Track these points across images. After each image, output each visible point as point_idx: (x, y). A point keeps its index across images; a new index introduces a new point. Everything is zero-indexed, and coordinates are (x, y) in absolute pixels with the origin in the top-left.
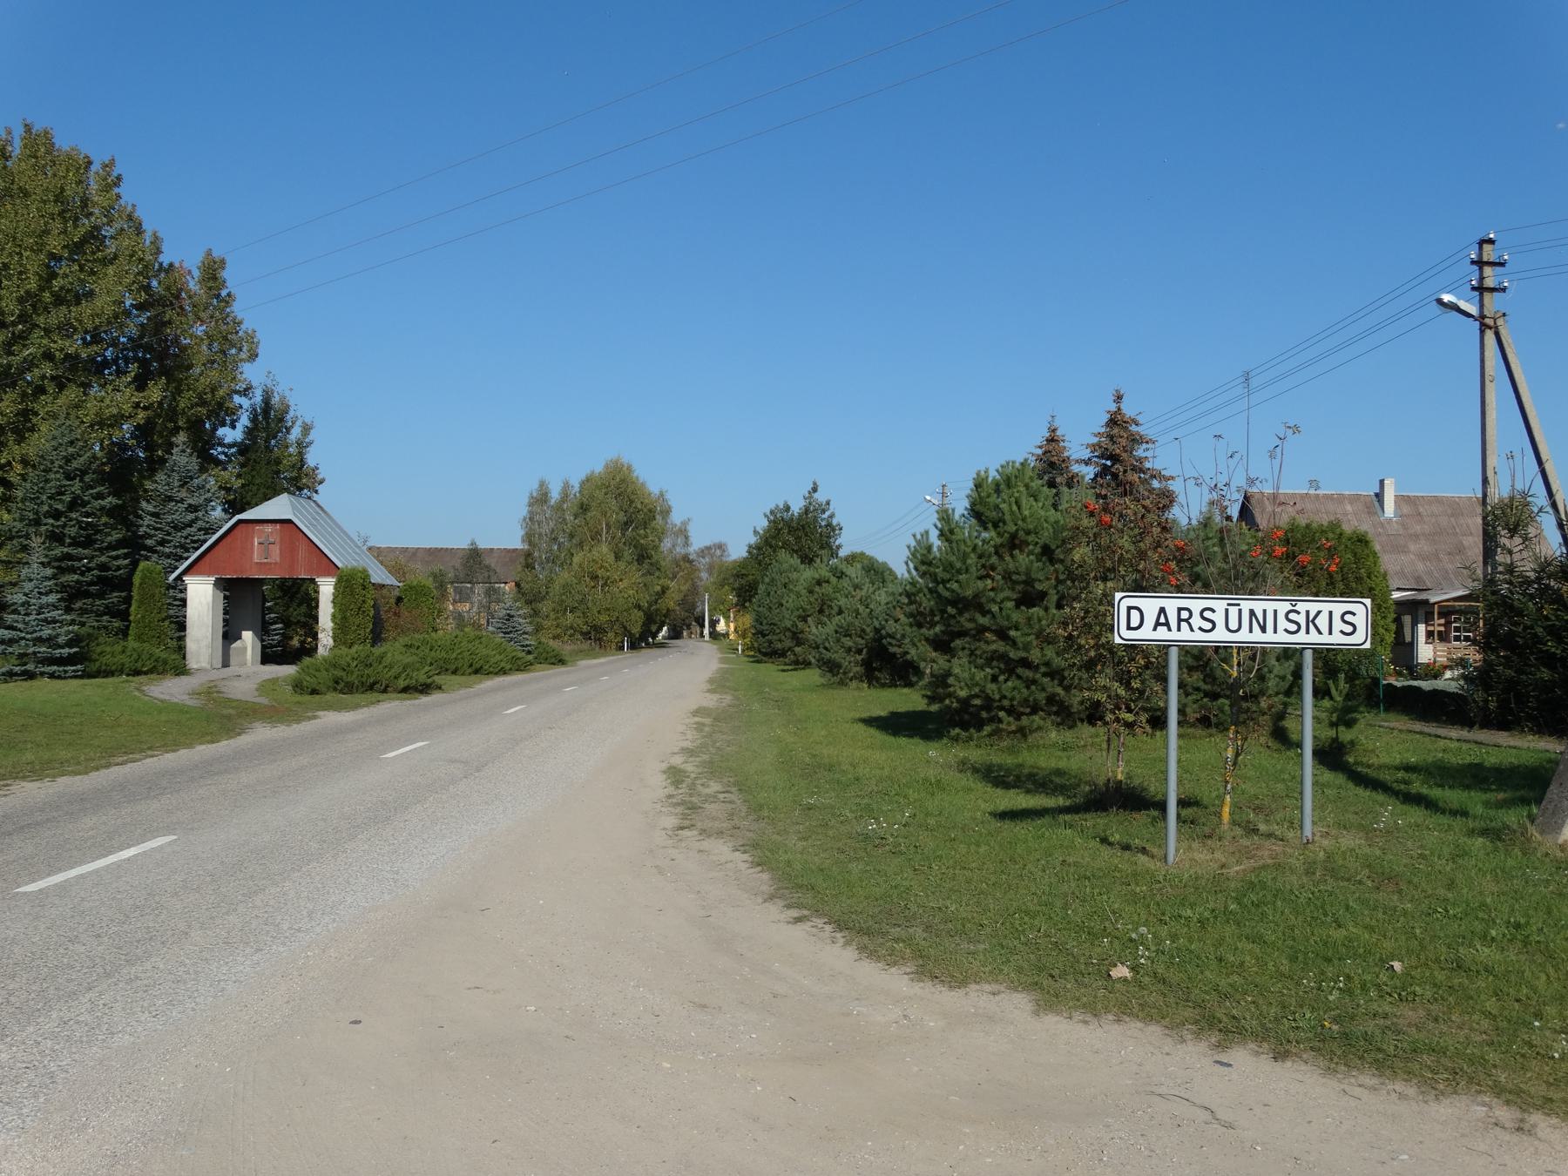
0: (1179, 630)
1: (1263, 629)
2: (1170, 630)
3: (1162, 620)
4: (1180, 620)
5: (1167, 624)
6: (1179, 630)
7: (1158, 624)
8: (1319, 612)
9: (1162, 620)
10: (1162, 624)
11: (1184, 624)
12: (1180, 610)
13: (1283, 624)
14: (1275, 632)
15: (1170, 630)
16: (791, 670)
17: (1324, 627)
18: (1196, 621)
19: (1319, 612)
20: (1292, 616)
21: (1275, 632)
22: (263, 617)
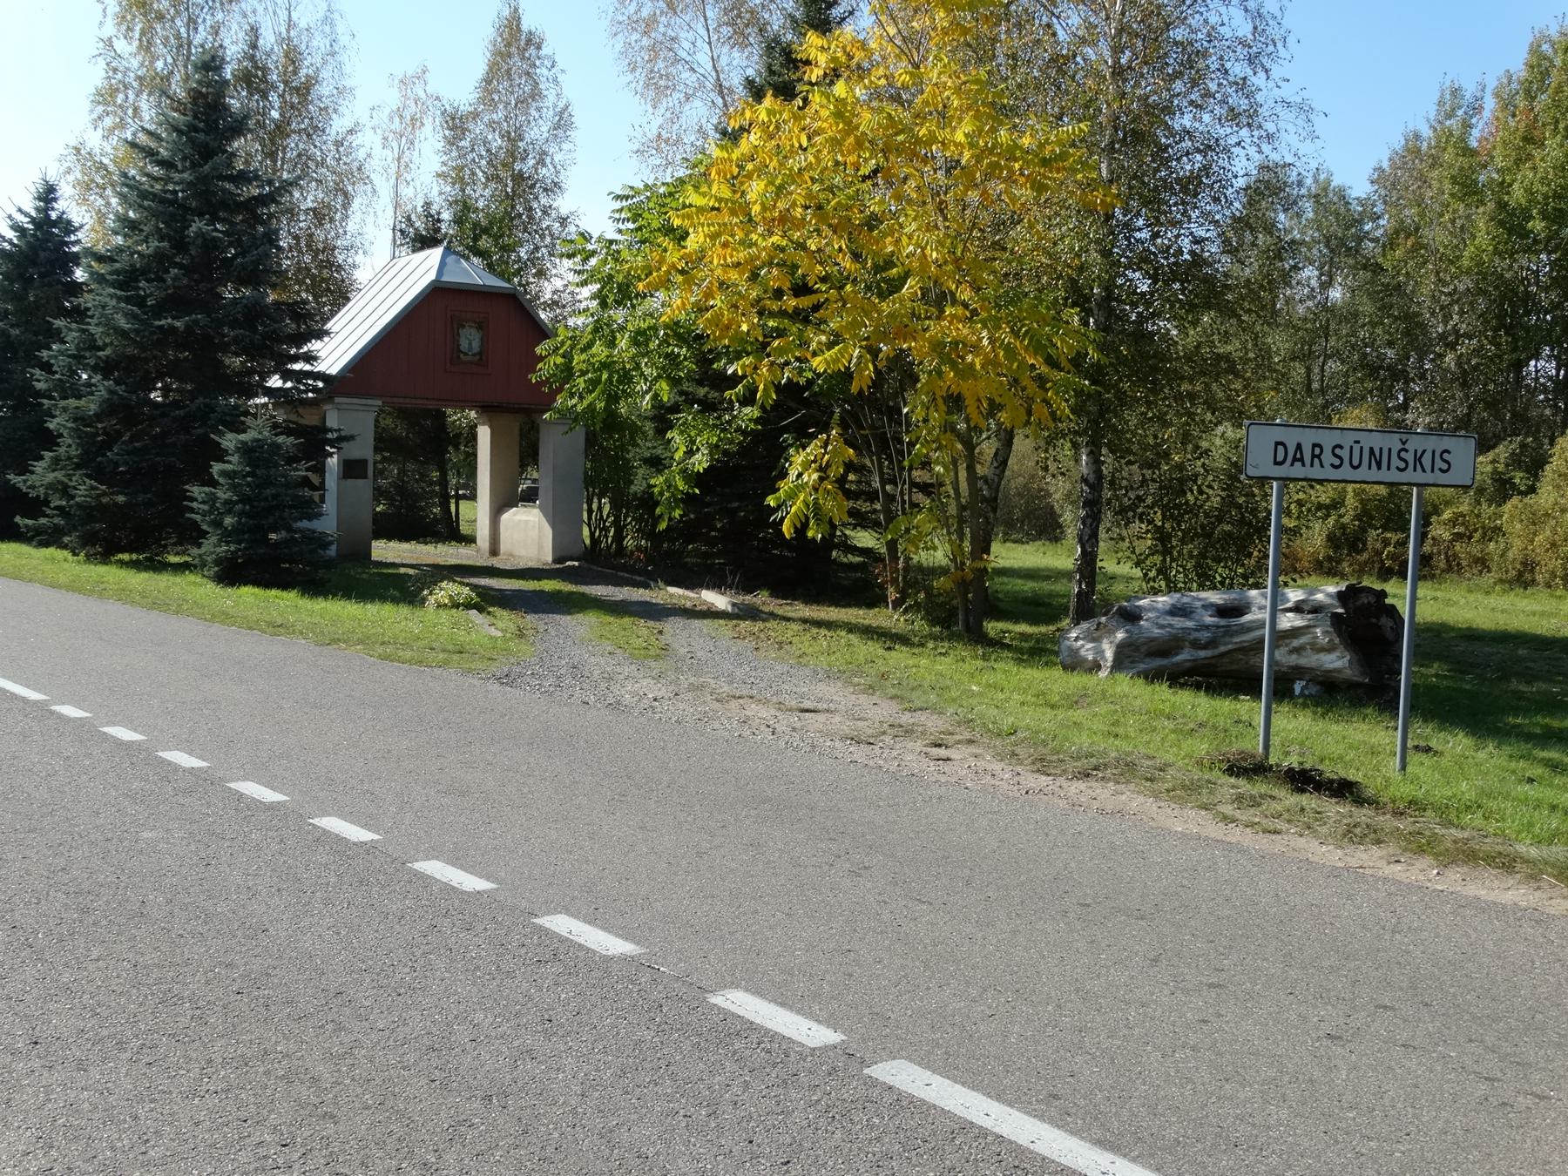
0: (1312, 465)
1: (1379, 467)
2: (1303, 465)
3: (1298, 456)
4: (1314, 456)
5: (1302, 460)
6: (1312, 465)
7: (1295, 460)
8: (1424, 451)
9: (1298, 456)
10: (1298, 460)
11: (1316, 460)
12: (1314, 446)
13: (1395, 462)
14: (1389, 469)
15: (1303, 465)
16: (404, 565)
17: (1428, 466)
18: (1328, 458)
19: (1424, 451)
20: (1403, 454)
21: (1389, 469)
22: (1414, 485)
